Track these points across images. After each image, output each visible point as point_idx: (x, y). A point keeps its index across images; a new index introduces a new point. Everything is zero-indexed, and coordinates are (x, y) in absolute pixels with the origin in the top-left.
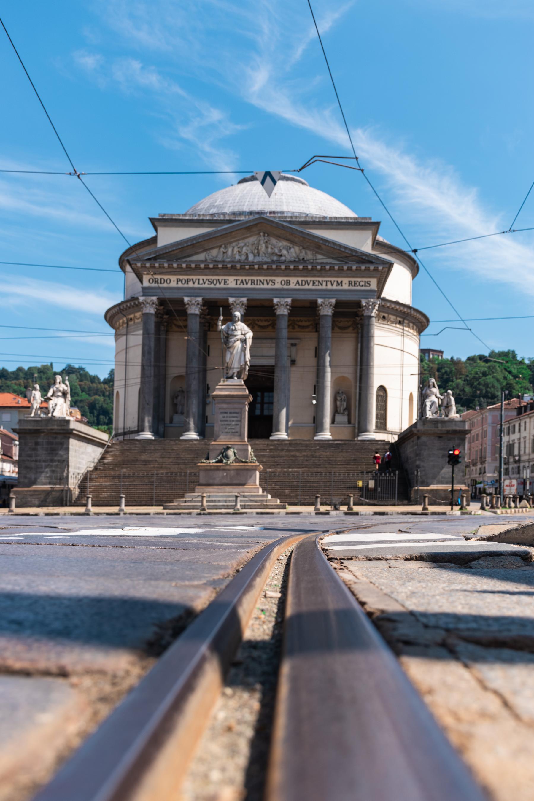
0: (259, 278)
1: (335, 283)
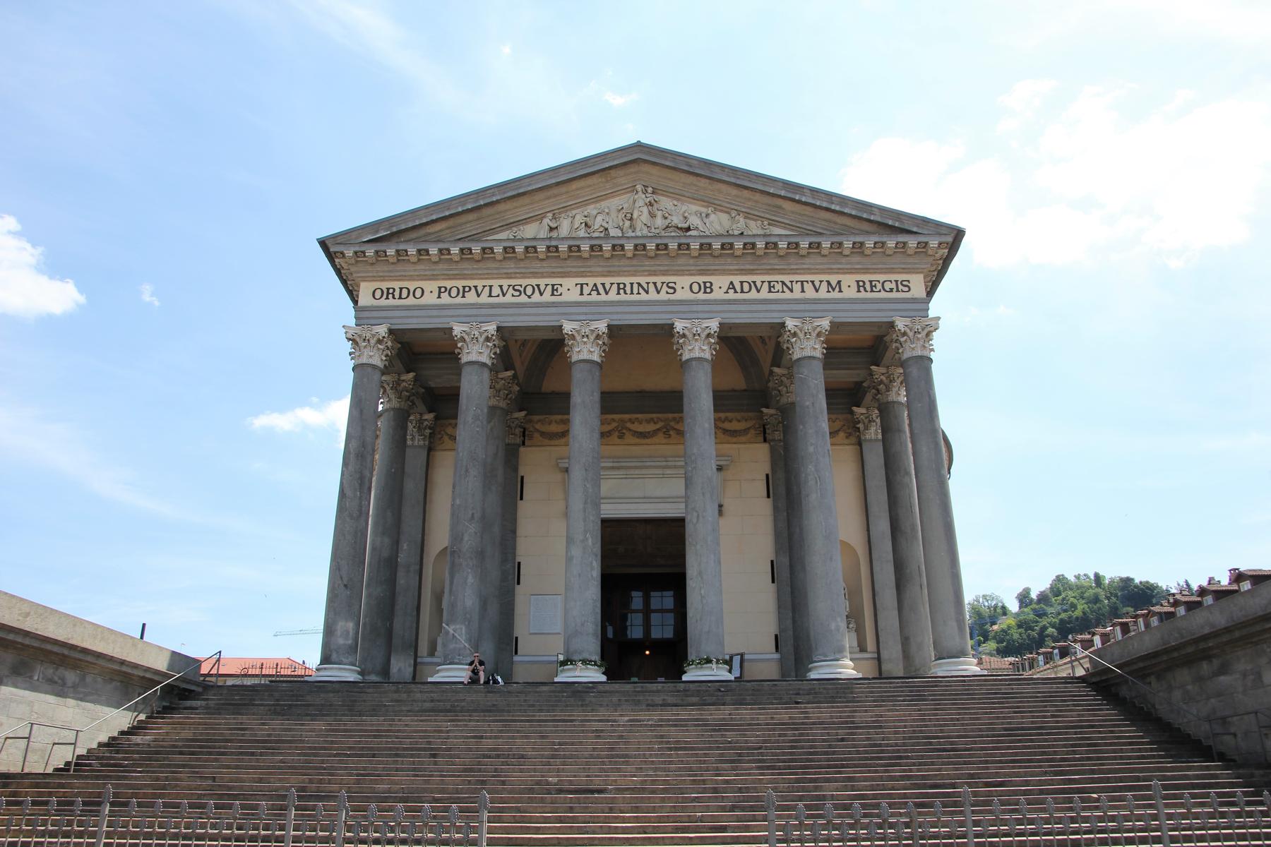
0: (635, 280)
1: (824, 285)
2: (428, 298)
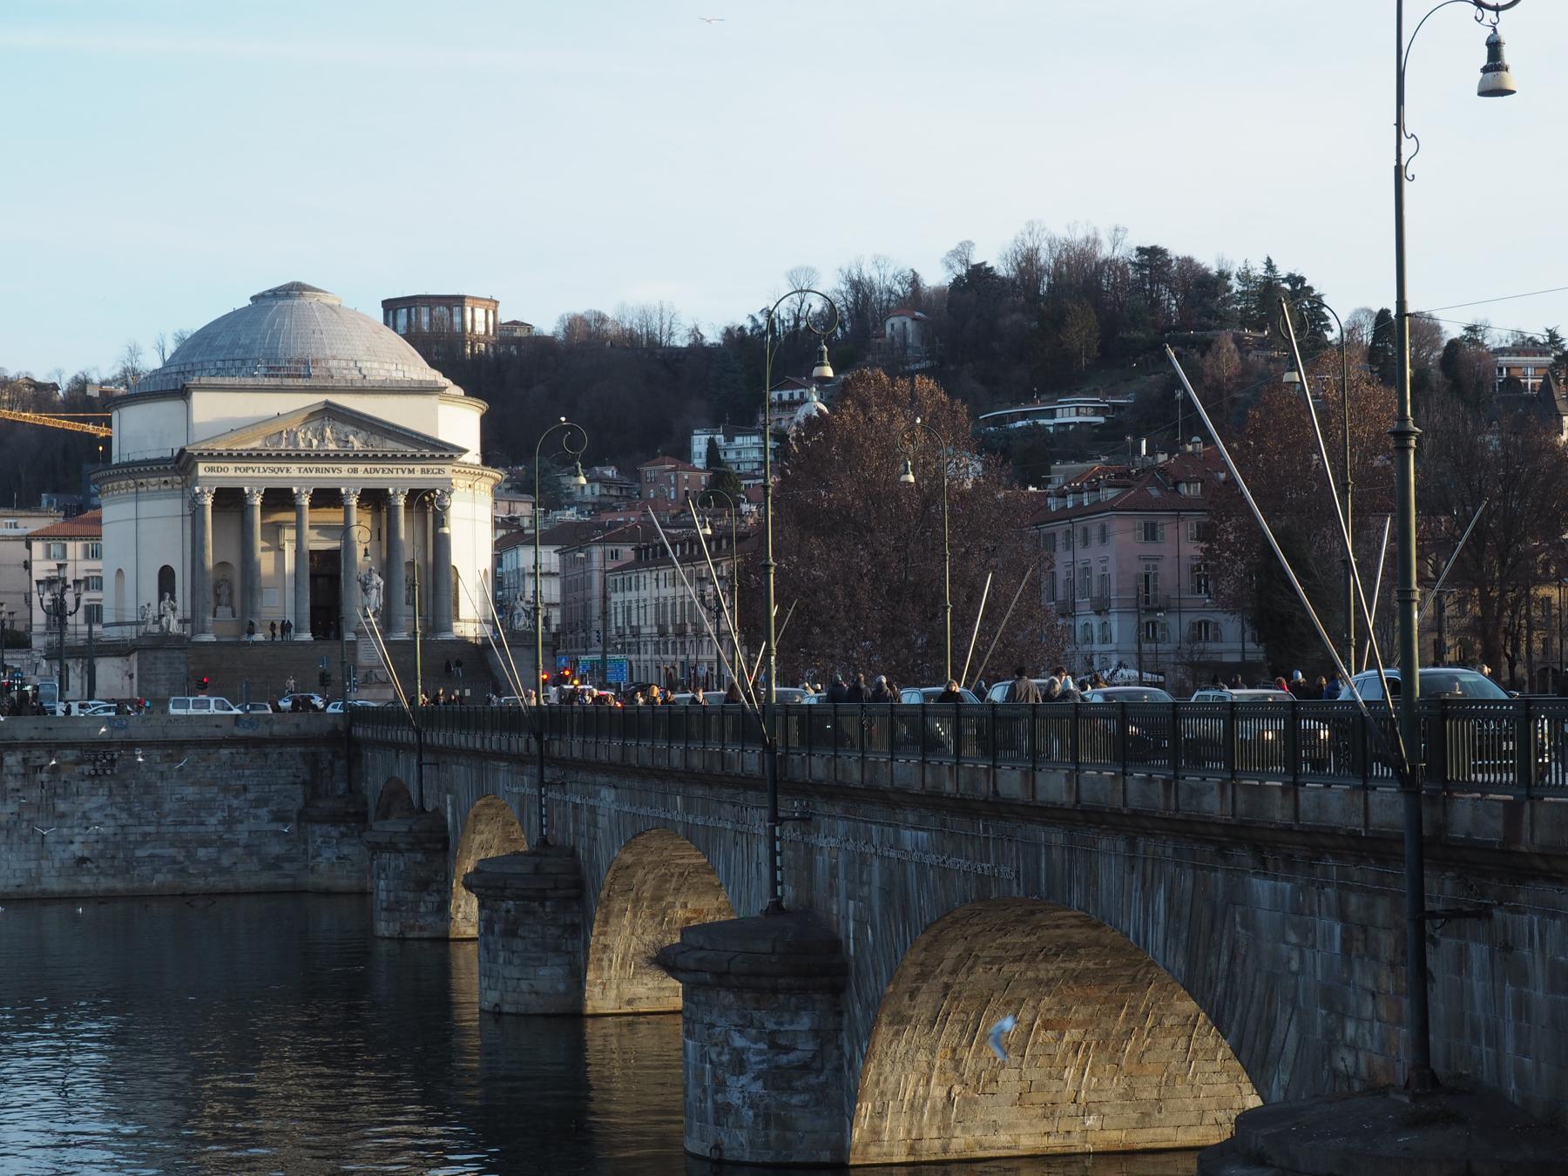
2: (230, 473)
